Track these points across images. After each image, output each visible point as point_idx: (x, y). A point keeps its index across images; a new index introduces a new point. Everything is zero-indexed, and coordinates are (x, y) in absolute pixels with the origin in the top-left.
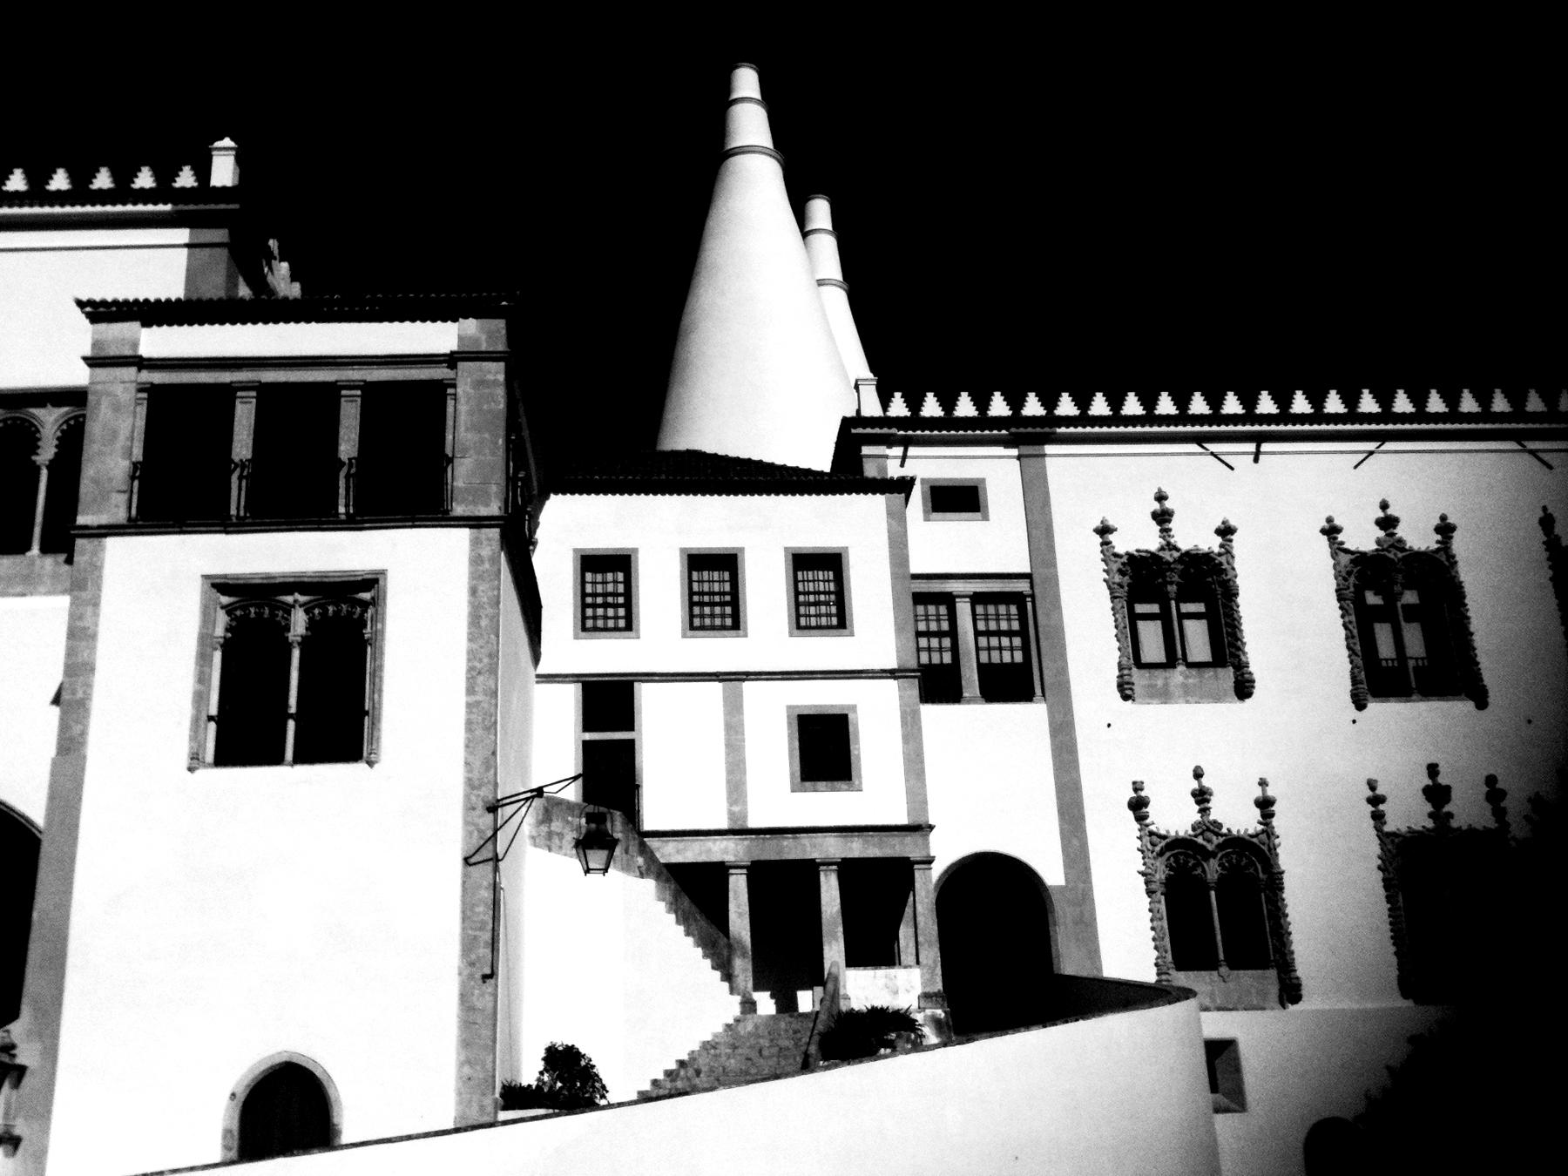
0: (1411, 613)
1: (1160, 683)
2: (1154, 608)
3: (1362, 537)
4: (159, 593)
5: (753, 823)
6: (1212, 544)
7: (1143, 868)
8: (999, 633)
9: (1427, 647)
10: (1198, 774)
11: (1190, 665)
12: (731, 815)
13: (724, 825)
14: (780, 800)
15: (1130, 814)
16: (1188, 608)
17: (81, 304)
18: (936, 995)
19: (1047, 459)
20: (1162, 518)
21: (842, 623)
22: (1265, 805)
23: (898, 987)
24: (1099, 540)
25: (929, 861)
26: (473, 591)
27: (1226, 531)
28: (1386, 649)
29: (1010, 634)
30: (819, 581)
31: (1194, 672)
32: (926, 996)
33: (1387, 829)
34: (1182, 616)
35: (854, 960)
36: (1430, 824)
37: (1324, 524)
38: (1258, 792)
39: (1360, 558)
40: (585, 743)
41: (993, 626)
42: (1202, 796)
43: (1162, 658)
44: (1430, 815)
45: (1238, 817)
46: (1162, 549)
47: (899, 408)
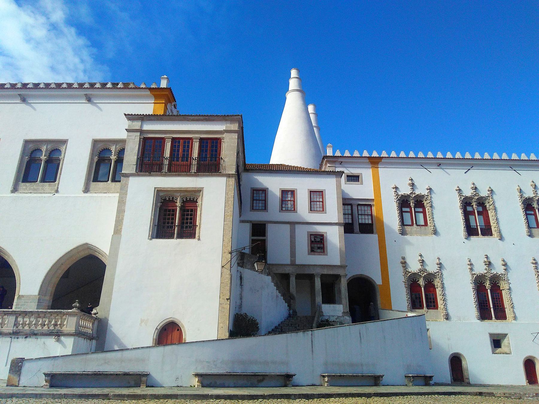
1: (409, 230)
2: (408, 210)
3: (468, 192)
4: (142, 192)
5: (298, 262)
6: (425, 192)
7: (404, 281)
10: (421, 256)
11: (417, 225)
12: (291, 260)
13: (289, 262)
14: (305, 257)
17: (125, 115)
18: (347, 312)
21: (323, 210)
23: (335, 310)
24: (394, 190)
25: (346, 275)
26: (227, 194)
28: (473, 223)
29: (368, 215)
30: (316, 198)
31: (419, 227)
32: (344, 313)
33: (473, 273)
35: (324, 302)
36: (485, 272)
39: (466, 198)
40: (252, 240)
41: (363, 213)
43: (411, 224)
44: (486, 269)
47: (338, 154)
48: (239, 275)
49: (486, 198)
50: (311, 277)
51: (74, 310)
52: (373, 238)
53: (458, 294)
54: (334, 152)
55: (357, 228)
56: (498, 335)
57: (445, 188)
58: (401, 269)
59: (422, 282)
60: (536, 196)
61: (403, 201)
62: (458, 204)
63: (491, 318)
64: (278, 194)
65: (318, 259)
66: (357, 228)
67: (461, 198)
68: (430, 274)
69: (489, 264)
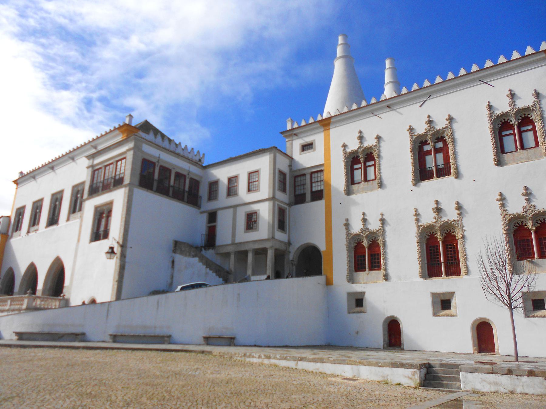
0: (437, 151)
8: (318, 182)
9: (444, 162)
10: (364, 214)
13: (230, 242)
15: (344, 227)
16: (368, 164)
19: (331, 130)
20: (361, 138)
22: (383, 221)
27: (379, 138)
31: (366, 183)
33: (420, 224)
34: (366, 167)
36: (434, 220)
37: (408, 128)
38: (380, 217)
39: (419, 136)
42: (364, 220)
44: (435, 218)
45: (374, 225)
46: (358, 149)
47: (296, 126)
48: (171, 260)
49: (443, 131)
50: (245, 253)
51: (27, 295)
52: (320, 204)
53: (403, 252)
54: (292, 125)
55: (308, 196)
56: (444, 294)
57: (393, 131)
58: (345, 232)
59: (365, 243)
60: (512, 110)
61: (354, 158)
62: (407, 145)
63: (440, 275)
64: (226, 181)
65: (253, 236)
66: (308, 196)
67: (412, 138)
68: (372, 233)
69: (438, 210)
